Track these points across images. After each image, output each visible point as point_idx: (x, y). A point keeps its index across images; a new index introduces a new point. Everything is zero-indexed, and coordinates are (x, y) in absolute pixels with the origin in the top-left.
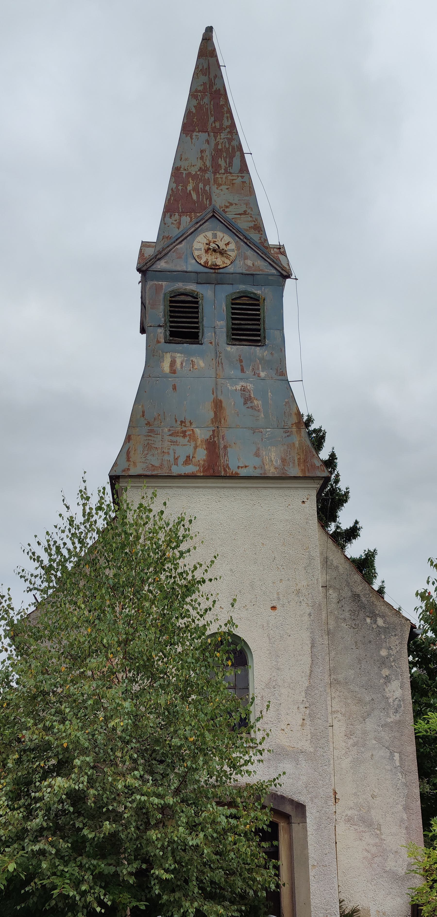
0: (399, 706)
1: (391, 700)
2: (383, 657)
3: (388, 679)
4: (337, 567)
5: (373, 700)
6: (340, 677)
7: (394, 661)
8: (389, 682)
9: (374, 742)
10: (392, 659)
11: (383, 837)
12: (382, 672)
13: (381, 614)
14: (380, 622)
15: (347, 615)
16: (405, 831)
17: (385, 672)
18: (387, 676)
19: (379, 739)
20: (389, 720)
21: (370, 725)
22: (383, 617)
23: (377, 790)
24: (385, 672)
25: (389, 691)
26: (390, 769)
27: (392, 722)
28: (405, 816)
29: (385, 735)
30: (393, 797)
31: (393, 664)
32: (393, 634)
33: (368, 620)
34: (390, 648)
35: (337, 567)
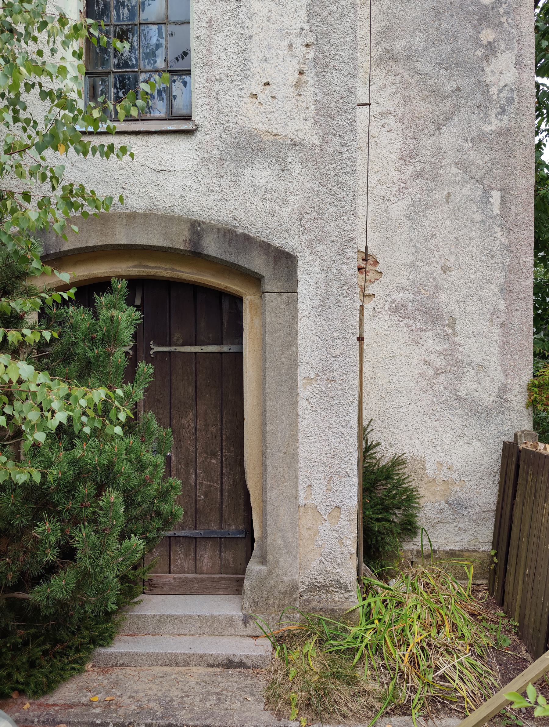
0: (510, 101)
1: (494, 90)
3: (491, 49)
5: (459, 89)
6: (399, 46)
8: (494, 55)
9: (454, 170)
11: (457, 339)
12: (481, 36)
16: (498, 331)
17: (488, 35)
18: (490, 43)
19: (463, 166)
20: (487, 128)
21: (449, 138)
23: (452, 258)
25: (492, 71)
26: (480, 220)
27: (493, 132)
28: (502, 305)
29: (477, 158)
30: (481, 269)
31: (503, 20)
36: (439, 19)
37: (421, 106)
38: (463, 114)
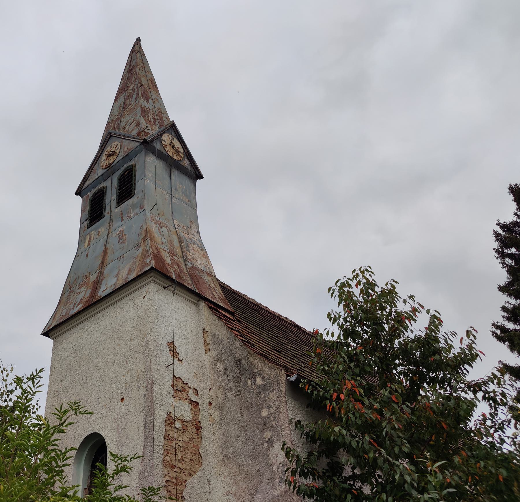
1: (275, 468)
2: (265, 418)
3: (270, 443)
4: (222, 339)
5: (259, 471)
6: (230, 451)
7: (274, 419)
8: (272, 445)
10: (272, 418)
12: (265, 436)
13: (259, 372)
14: (259, 381)
15: (232, 382)
17: (268, 434)
20: (276, 493)
22: (260, 374)
24: (268, 434)
25: (272, 456)
27: (279, 495)
31: (273, 424)
32: (271, 389)
33: (249, 382)
34: (270, 407)
35: (222, 339)
36: (245, 432)
37: (243, 485)
38: (263, 486)
